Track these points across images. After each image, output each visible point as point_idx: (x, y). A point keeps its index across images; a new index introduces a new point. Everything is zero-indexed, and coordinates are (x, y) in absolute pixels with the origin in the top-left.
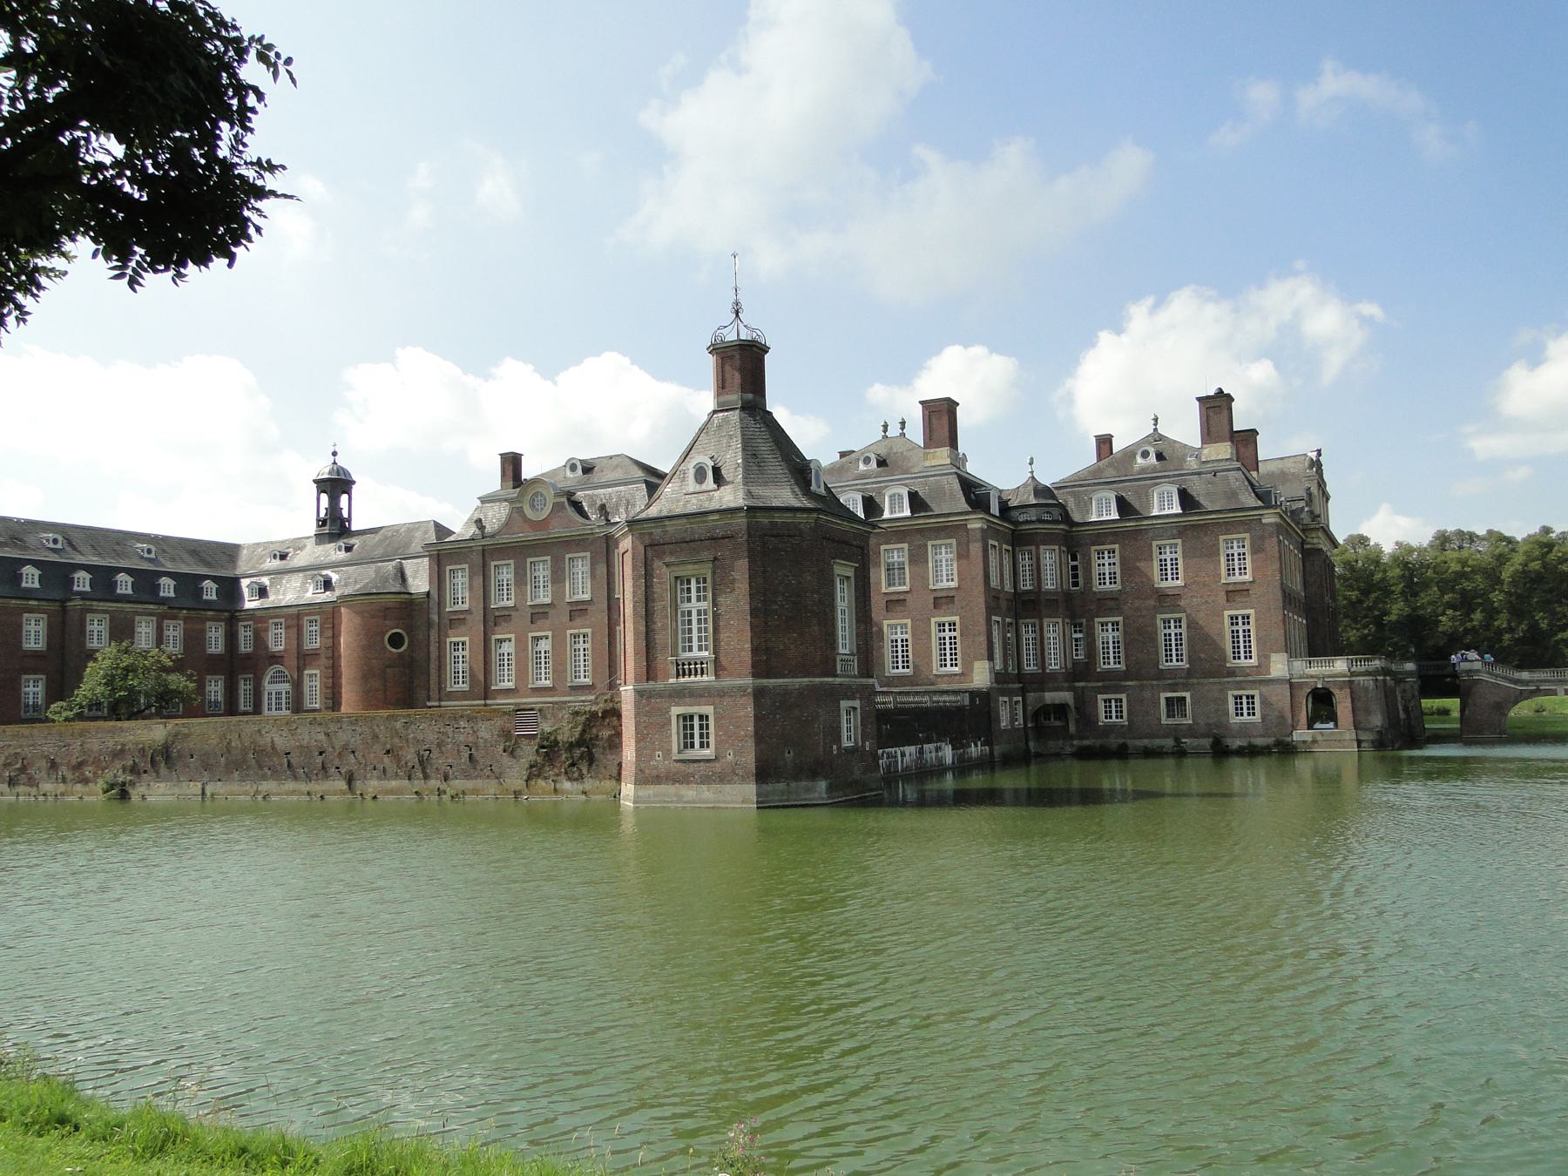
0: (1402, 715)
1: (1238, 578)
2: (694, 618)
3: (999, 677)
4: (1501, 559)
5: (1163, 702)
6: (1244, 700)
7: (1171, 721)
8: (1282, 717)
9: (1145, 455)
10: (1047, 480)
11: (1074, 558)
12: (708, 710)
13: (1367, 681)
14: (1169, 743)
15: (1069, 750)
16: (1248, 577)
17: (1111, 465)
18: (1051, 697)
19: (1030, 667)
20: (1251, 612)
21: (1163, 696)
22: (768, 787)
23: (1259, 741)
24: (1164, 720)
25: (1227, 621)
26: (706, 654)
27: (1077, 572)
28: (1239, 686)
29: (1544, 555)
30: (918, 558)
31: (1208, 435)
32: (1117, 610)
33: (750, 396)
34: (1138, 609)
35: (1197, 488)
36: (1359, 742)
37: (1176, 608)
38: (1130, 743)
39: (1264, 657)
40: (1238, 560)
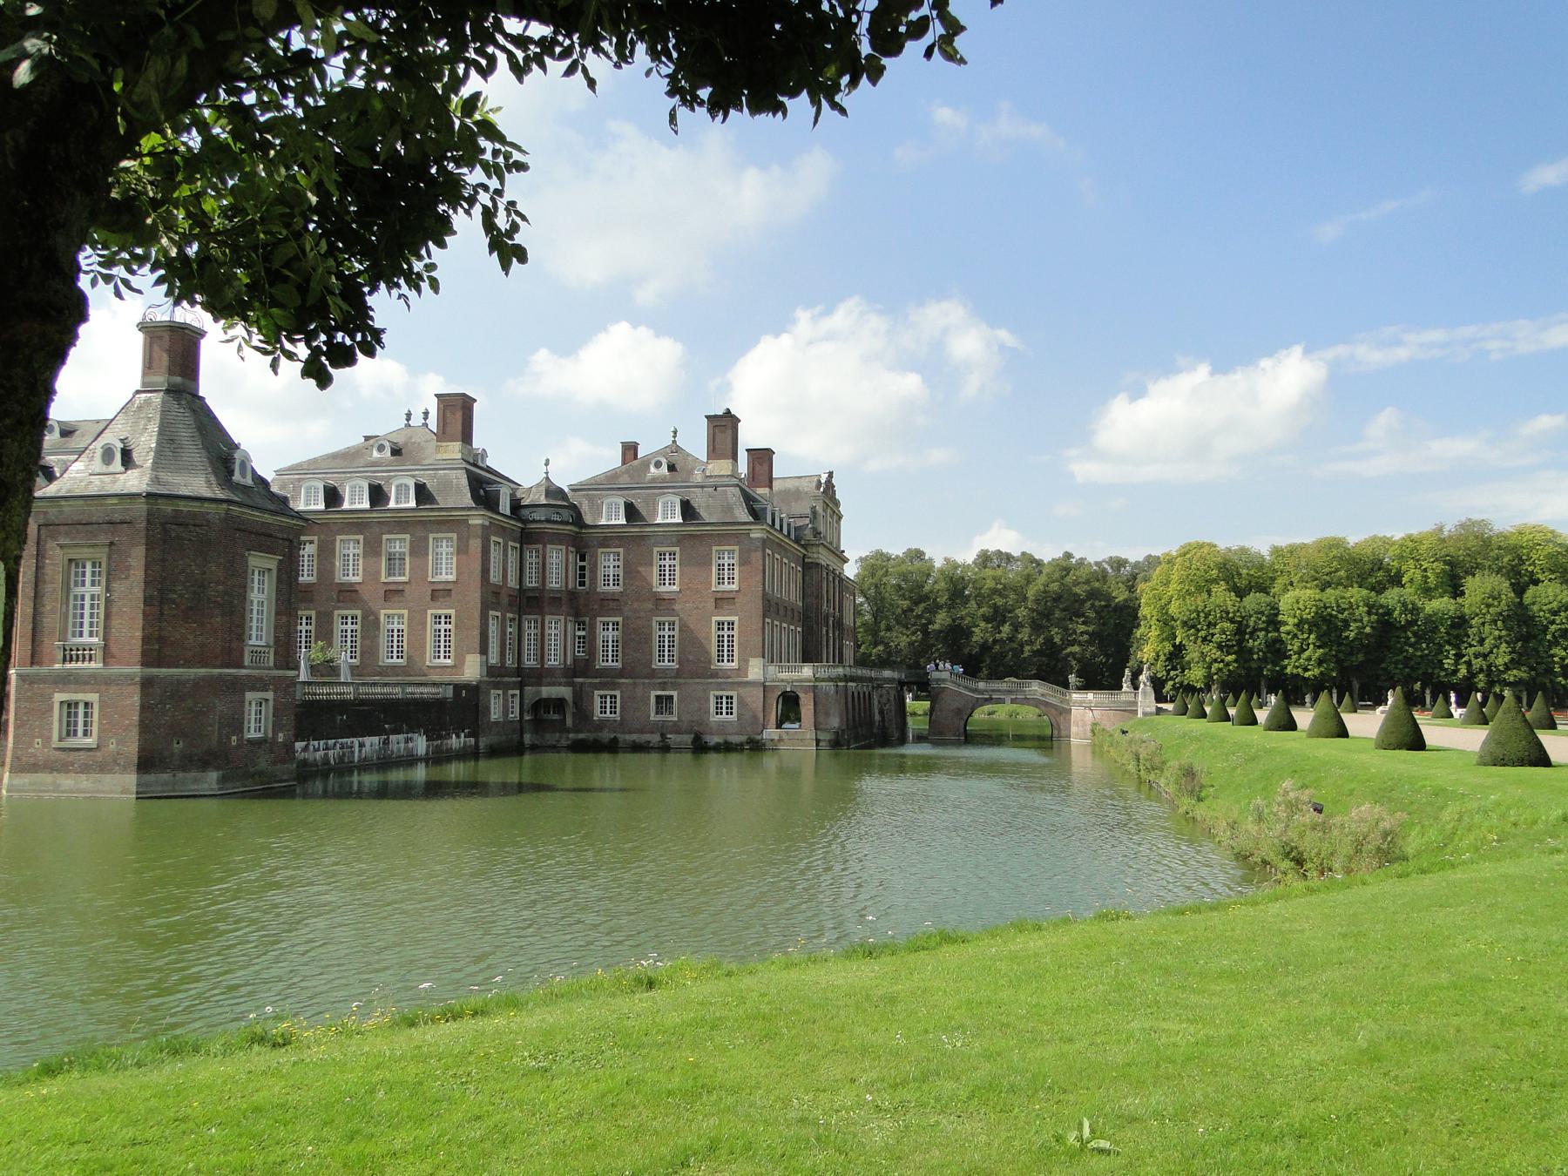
0: (877, 717)
1: (726, 587)
2: (87, 602)
3: (491, 671)
4: (1029, 579)
5: (653, 700)
7: (659, 718)
8: (755, 717)
9: (658, 465)
10: (563, 483)
11: (583, 559)
12: (93, 697)
14: (655, 738)
15: (564, 743)
16: (735, 587)
17: (627, 471)
18: (547, 691)
19: (530, 662)
20: (735, 619)
21: (653, 694)
22: (151, 778)
23: (735, 739)
24: (653, 717)
25: (714, 627)
26: (95, 640)
28: (720, 687)
30: (419, 550)
31: (714, 452)
33: (178, 379)
34: (635, 611)
35: (699, 501)
36: (818, 741)
37: (672, 612)
38: (621, 737)
39: (744, 661)
40: (728, 572)
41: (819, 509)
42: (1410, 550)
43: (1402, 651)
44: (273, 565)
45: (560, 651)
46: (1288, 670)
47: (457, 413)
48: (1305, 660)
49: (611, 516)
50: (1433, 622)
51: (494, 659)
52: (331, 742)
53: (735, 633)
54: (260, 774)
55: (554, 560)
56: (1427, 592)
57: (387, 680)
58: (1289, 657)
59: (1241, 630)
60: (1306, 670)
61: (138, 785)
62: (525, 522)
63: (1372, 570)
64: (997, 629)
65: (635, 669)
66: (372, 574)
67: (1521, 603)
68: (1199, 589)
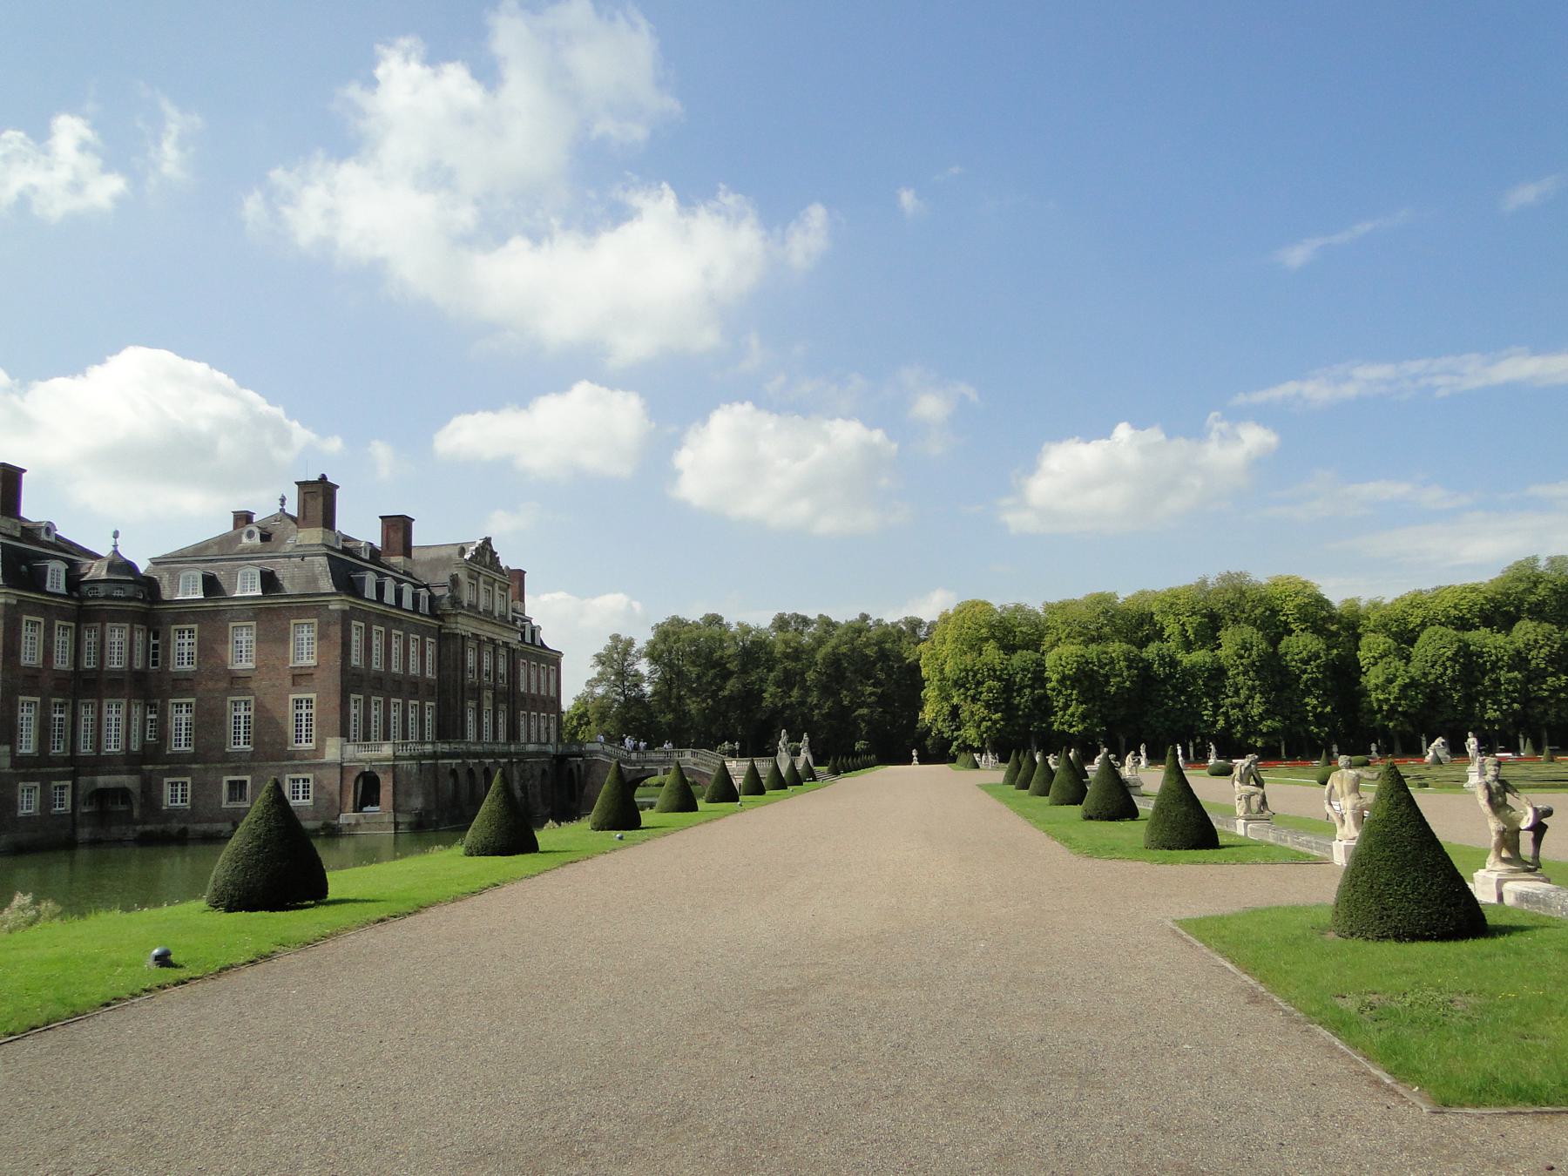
4: (820, 642)
5: (225, 786)
7: (233, 805)
8: (332, 801)
13: (410, 765)
15: (131, 835)
18: (102, 781)
19: (85, 749)
20: (313, 696)
27: (157, 653)
28: (296, 769)
29: (852, 639)
36: (396, 825)
37: (246, 691)
39: (321, 742)
41: (463, 576)
42: (1172, 602)
43: (1163, 704)
45: (122, 740)
46: (1055, 727)
48: (1069, 716)
49: (189, 590)
50: (1192, 673)
51: (28, 745)
53: (313, 711)
55: (116, 639)
56: (1188, 646)
58: (1055, 714)
59: (1009, 687)
60: (1071, 726)
62: (82, 598)
63: (1138, 625)
64: (787, 694)
65: (209, 753)
67: (1275, 653)
68: (972, 647)
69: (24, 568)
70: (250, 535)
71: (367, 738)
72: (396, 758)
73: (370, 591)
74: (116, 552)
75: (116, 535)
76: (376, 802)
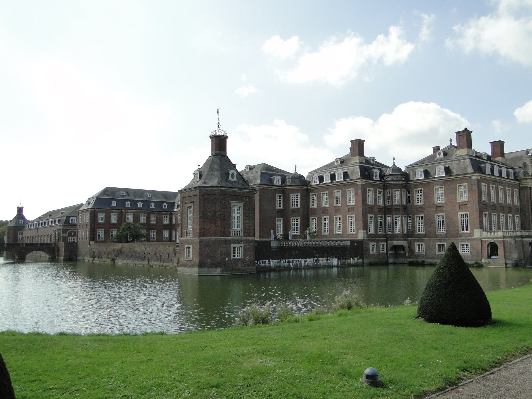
3: (369, 236)
5: (437, 246)
6: (465, 246)
13: (512, 241)
15: (406, 262)
18: (395, 243)
19: (389, 232)
20: (468, 213)
21: (437, 244)
22: (202, 270)
24: (437, 253)
25: (459, 216)
27: (409, 199)
28: (463, 241)
30: (344, 195)
32: (422, 212)
33: (218, 152)
36: (506, 264)
37: (442, 211)
38: (425, 260)
44: (242, 205)
47: (358, 146)
49: (419, 176)
51: (372, 231)
52: (291, 260)
53: (468, 218)
54: (238, 269)
55: (396, 195)
57: (336, 239)
61: (199, 272)
65: (430, 234)
66: (331, 204)
69: (366, 172)
70: (440, 154)
71: (491, 229)
72: (504, 237)
73: (488, 171)
74: (394, 165)
75: (394, 159)
76: (497, 255)
